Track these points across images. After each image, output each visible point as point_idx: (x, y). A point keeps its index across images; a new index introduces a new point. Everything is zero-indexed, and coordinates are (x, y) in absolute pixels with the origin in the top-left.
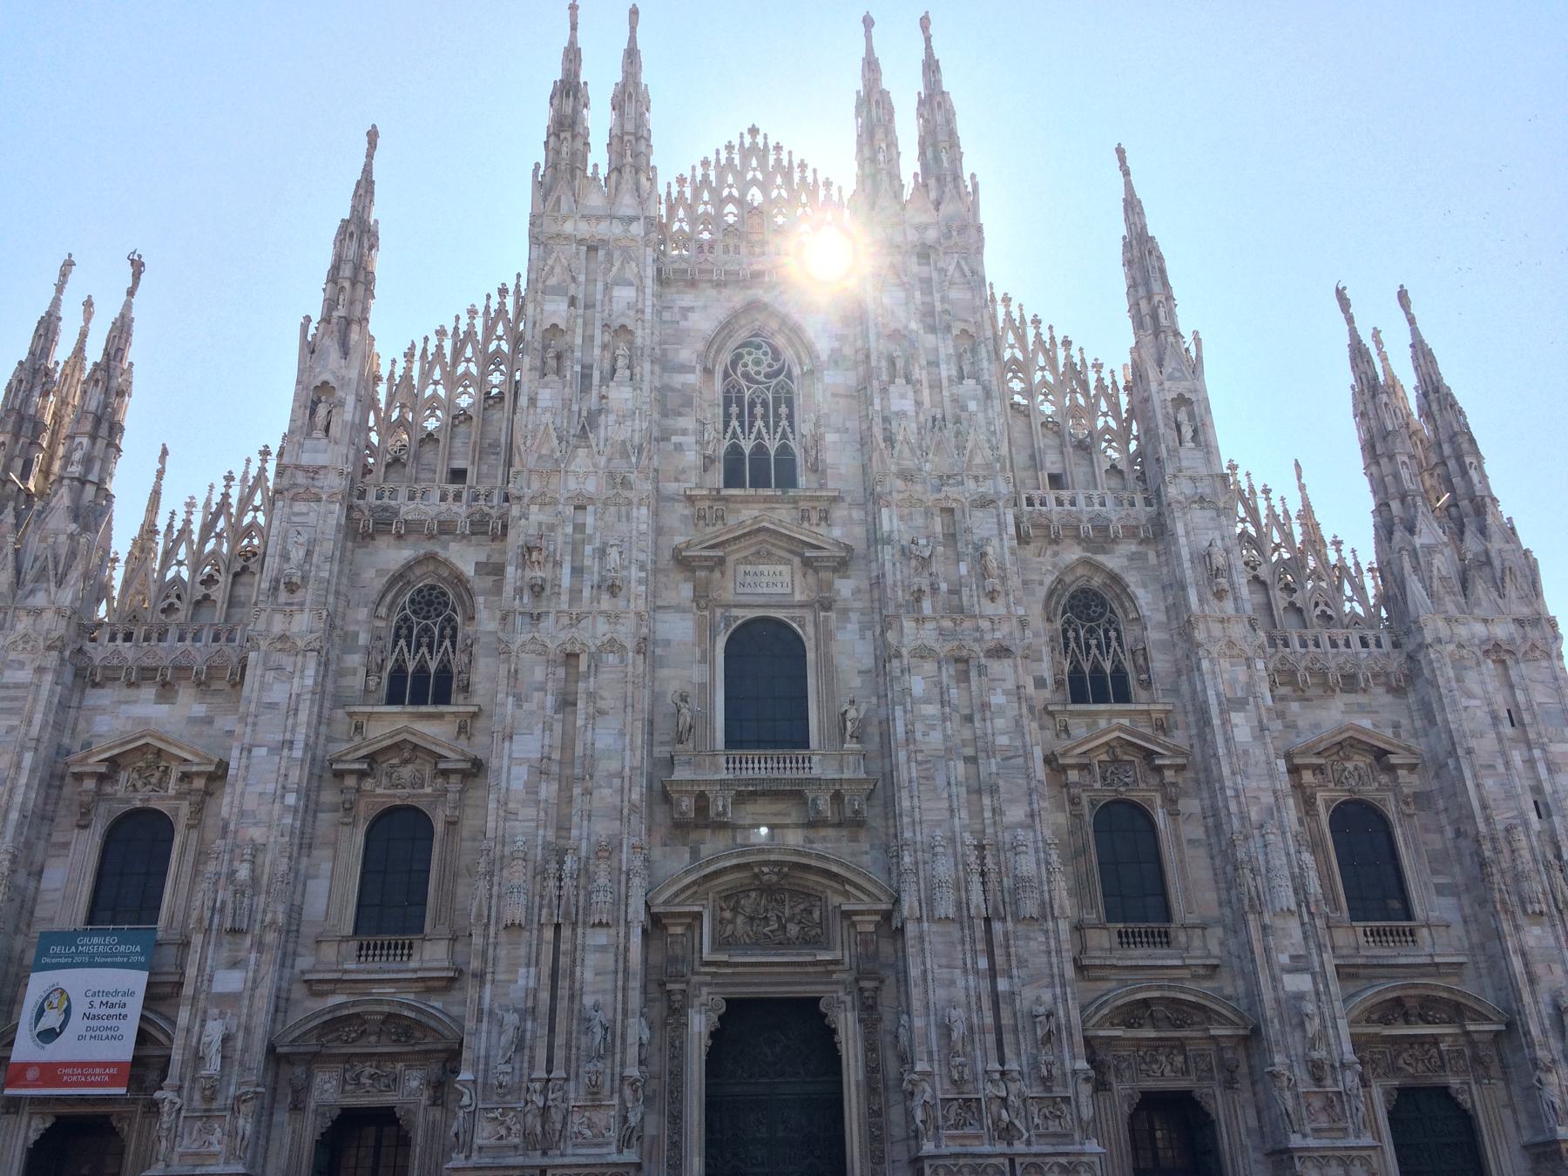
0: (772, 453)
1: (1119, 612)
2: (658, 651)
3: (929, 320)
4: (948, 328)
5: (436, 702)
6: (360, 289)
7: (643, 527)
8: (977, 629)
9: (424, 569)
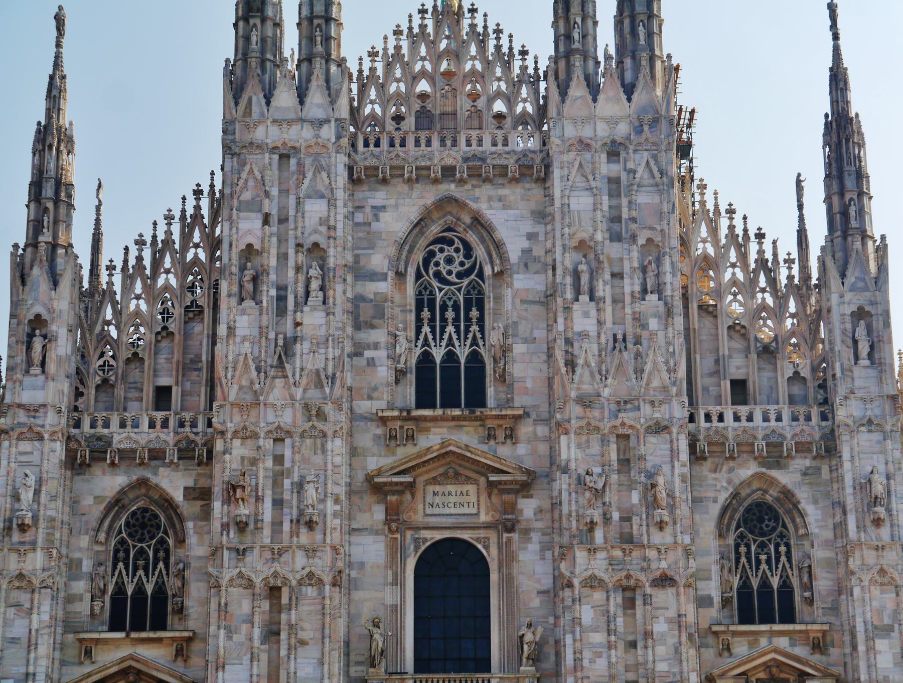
0: (463, 361)
1: (790, 526)
2: (354, 574)
3: (616, 226)
4: (634, 238)
5: (154, 628)
6: (63, 209)
7: (338, 460)
8: (645, 559)
9: (138, 492)
